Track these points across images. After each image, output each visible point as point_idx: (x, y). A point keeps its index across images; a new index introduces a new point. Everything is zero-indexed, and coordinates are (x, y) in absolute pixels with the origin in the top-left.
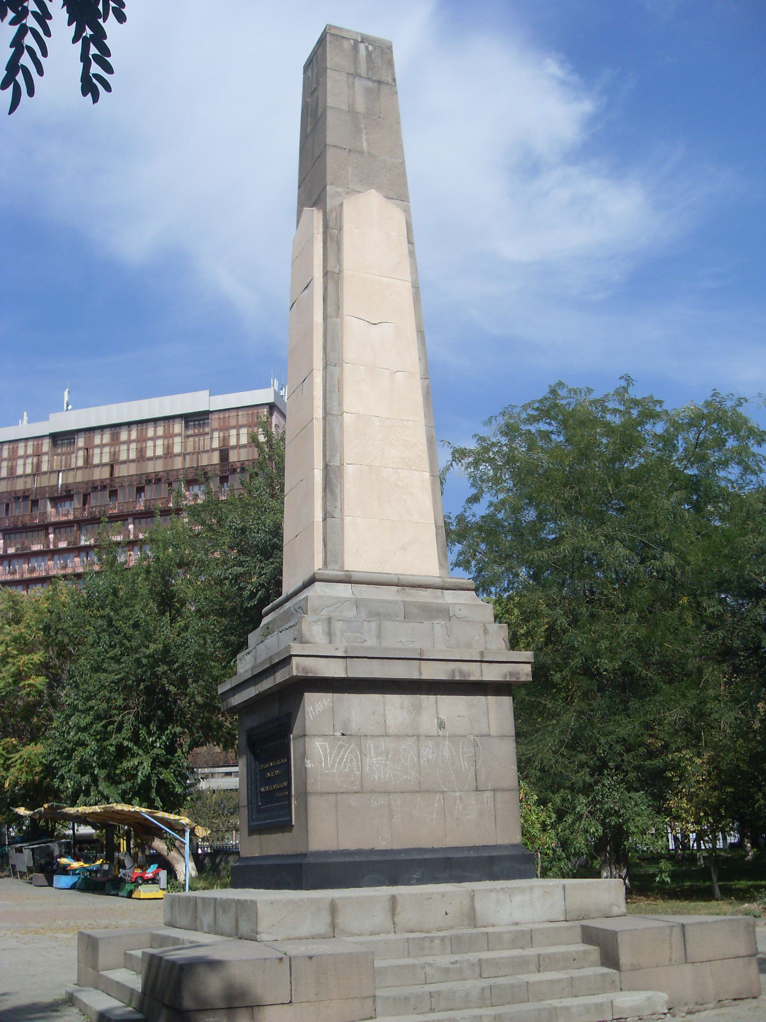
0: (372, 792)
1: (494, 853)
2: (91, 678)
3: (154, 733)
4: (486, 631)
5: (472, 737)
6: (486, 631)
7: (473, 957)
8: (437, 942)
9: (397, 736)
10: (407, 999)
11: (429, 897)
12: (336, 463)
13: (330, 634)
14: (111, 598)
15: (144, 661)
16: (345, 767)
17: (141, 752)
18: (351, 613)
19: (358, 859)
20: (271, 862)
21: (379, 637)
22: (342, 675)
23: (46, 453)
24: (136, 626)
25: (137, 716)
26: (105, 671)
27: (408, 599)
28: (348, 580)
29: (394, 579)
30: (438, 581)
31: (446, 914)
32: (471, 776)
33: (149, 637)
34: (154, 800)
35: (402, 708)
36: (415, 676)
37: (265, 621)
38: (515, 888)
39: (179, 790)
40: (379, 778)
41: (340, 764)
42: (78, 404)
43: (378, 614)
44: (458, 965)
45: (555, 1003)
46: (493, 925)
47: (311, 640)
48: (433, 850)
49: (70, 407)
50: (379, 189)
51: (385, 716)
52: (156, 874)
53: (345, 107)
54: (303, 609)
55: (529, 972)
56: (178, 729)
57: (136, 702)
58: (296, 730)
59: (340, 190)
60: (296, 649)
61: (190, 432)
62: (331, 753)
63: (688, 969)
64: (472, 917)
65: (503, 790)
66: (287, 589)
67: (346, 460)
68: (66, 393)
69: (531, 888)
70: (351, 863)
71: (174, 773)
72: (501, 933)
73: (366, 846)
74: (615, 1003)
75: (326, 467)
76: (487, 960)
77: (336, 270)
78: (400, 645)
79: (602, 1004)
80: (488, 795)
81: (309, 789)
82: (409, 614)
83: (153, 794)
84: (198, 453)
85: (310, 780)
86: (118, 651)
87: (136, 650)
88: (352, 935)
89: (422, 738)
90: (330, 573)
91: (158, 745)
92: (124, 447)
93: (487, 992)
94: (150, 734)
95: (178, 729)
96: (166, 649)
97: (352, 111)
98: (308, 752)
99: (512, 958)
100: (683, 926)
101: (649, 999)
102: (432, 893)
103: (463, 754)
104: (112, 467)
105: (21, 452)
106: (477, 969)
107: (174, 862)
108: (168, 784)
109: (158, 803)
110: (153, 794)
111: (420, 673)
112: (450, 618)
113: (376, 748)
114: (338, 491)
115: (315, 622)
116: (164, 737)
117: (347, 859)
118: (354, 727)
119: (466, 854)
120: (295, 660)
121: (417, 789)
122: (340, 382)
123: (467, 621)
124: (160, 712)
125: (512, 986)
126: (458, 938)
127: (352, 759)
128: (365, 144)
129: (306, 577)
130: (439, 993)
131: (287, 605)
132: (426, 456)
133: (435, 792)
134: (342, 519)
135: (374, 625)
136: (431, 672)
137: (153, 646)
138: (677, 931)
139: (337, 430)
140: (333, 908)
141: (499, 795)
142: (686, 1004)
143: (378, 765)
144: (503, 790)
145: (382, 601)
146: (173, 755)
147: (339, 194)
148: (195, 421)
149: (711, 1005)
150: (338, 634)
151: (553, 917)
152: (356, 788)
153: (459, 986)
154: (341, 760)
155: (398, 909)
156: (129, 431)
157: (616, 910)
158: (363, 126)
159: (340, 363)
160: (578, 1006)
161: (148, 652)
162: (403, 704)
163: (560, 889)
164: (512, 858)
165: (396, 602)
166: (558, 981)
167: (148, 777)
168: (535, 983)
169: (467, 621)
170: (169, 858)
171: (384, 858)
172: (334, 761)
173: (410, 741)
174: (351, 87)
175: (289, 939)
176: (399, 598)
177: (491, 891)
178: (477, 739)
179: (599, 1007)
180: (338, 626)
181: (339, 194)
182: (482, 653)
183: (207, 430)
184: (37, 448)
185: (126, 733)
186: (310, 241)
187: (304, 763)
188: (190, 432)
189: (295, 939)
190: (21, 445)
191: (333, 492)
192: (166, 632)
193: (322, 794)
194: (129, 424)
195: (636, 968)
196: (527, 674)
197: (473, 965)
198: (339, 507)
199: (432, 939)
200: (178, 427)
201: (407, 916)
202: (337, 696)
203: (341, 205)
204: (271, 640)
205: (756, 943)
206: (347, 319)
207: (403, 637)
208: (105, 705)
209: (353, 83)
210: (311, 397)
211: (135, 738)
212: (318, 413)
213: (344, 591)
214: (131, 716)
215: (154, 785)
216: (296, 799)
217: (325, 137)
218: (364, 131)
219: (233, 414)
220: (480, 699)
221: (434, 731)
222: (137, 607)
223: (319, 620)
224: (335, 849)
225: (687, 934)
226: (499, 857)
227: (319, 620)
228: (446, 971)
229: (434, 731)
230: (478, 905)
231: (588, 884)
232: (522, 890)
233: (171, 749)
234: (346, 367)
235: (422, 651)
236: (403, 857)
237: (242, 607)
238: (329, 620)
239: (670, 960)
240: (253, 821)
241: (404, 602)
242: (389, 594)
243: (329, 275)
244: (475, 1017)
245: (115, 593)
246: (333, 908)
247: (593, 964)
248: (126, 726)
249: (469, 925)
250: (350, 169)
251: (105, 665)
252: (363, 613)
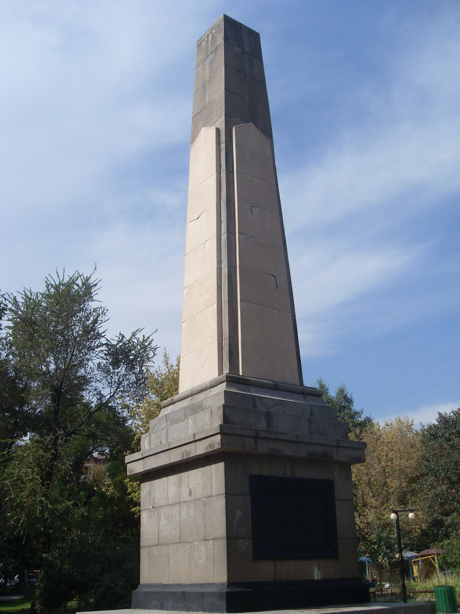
65: (218, 539)
80: (211, 542)
89: (182, 504)
113: (164, 514)
136: (175, 457)
141: (216, 542)
144: (218, 539)
152: (156, 542)
162: (174, 481)
226: (207, 593)
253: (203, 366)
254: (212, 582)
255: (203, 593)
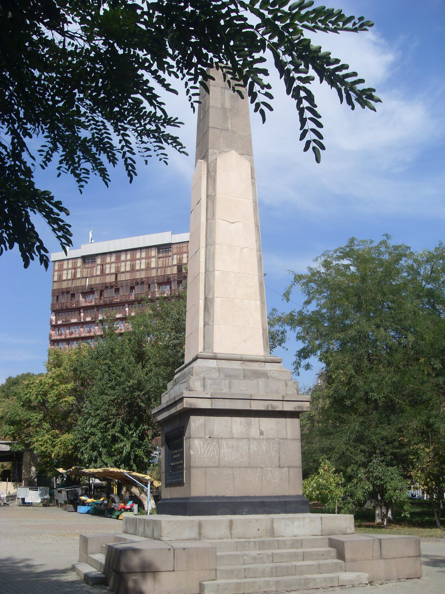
0: (224, 467)
1: (288, 500)
2: (98, 398)
3: (133, 429)
4: (286, 385)
5: (277, 440)
6: (286, 385)
7: (270, 552)
8: (252, 544)
9: (238, 439)
10: (232, 571)
11: (250, 521)
12: (210, 297)
13: (204, 386)
14: (110, 353)
15: (127, 389)
16: (211, 454)
17: (125, 439)
18: (216, 375)
19: (216, 501)
20: (174, 501)
21: (230, 387)
22: (210, 407)
23: (79, 267)
24: (123, 370)
25: (123, 419)
26: (106, 394)
27: (246, 368)
28: (215, 358)
29: (239, 357)
30: (263, 358)
31: (258, 530)
32: (277, 459)
33: (130, 376)
34: (132, 466)
35: (241, 424)
36: (248, 408)
37: (176, 377)
38: (295, 518)
39: (146, 460)
40: (228, 460)
41: (208, 452)
42: (98, 238)
43: (230, 376)
44: (261, 556)
45: (309, 576)
46: (283, 537)
47: (195, 389)
48: (255, 497)
49: (93, 241)
50: (236, 149)
51: (232, 428)
52: (132, 506)
53: (219, 106)
54: (191, 373)
55: (298, 560)
56: (146, 427)
57: (123, 411)
58: (187, 435)
59: (216, 151)
60: (186, 394)
61: (161, 255)
62: (203, 447)
63: (382, 562)
64: (272, 532)
65: (294, 467)
66: (187, 360)
67: (216, 296)
68: (91, 233)
69: (304, 518)
70: (212, 503)
71: (143, 451)
72: (285, 540)
73: (221, 494)
74: (340, 578)
75: (206, 298)
76: (276, 554)
77: (213, 195)
78: (241, 392)
79: (333, 578)
81: (192, 465)
82: (246, 376)
83: (132, 463)
84: (165, 267)
85: (192, 461)
86: (113, 383)
87: (123, 383)
88: (209, 539)
89: (251, 440)
90: (206, 354)
91: (135, 435)
92: (123, 264)
93: (274, 570)
94: (130, 429)
95: (146, 427)
96: (140, 383)
97: (223, 108)
98: (192, 446)
99: (289, 553)
100: (380, 540)
101: (358, 576)
102: (251, 519)
103: (273, 448)
104: (116, 275)
105: (65, 267)
106: (271, 558)
107: (143, 500)
108: (140, 457)
109: (135, 467)
110: (132, 463)
111: (250, 406)
112: (268, 378)
113: (227, 444)
114: (211, 311)
115: (197, 380)
116: (138, 431)
117: (210, 501)
118: (215, 434)
119: (273, 500)
120: (185, 399)
121: (248, 466)
122: (214, 254)
123: (277, 380)
124: (136, 417)
125: (287, 567)
126: (263, 542)
127: (214, 451)
128: (230, 126)
129: (194, 356)
130: (249, 569)
131: (186, 370)
132: (258, 292)
133: (257, 467)
134: (213, 326)
135: (227, 382)
137: (132, 381)
138: (377, 543)
139: (211, 279)
140: (200, 525)
141: (291, 469)
142: (380, 580)
143: (228, 453)
144: (294, 467)
145: (232, 369)
146: (143, 441)
147: (215, 153)
148: (163, 249)
149: (393, 581)
150: (208, 386)
151: (315, 533)
153: (260, 566)
154: (208, 451)
155: (234, 527)
156: (126, 255)
157: (349, 531)
158: (229, 116)
159: (213, 244)
160: (320, 578)
161: (129, 384)
162: (241, 422)
163: (319, 519)
164: (296, 502)
165: (240, 369)
166: (312, 565)
167: (129, 453)
168: (300, 566)
169: (277, 380)
170: (141, 498)
171: (229, 501)
172: (205, 451)
173: (245, 441)
174: (223, 94)
175: (177, 540)
176: (241, 367)
177: (282, 519)
178: (280, 441)
179: (331, 579)
180: (208, 382)
181: (215, 153)
182: (283, 396)
183: (170, 254)
184: (75, 264)
185: (117, 429)
186: (200, 178)
187: (189, 452)
188: (161, 255)
189: (180, 540)
190: (66, 262)
191: (208, 312)
192: (139, 373)
193: (198, 467)
194: (126, 251)
195: (353, 560)
196: (307, 407)
197: (269, 556)
198: (211, 320)
199: (249, 542)
200: (154, 253)
201: (238, 530)
202: (207, 418)
203: (216, 159)
204: (176, 388)
205: (420, 550)
206: (218, 220)
207: (242, 388)
208: (106, 413)
209: (224, 92)
210: (199, 262)
211: (122, 432)
212: (202, 270)
213: (213, 363)
214: (120, 419)
215: (132, 457)
216: (186, 470)
217: (208, 122)
218: (230, 119)
219: (185, 245)
220: (283, 420)
221: (257, 436)
222: (124, 360)
223: (198, 379)
224: (204, 495)
225: (382, 544)
227: (198, 379)
228: (255, 558)
229: (257, 436)
230: (275, 526)
231: (334, 516)
232: (299, 519)
233: (142, 437)
234: (217, 246)
235: (251, 395)
236: (239, 500)
237: (178, 362)
238: (204, 379)
239: (373, 557)
240: (167, 480)
241: (244, 369)
242: (236, 365)
243: (209, 197)
244: (266, 581)
245: (112, 350)
246: (200, 525)
247: (333, 558)
248: (118, 425)
249: (270, 536)
250: (221, 139)
251: (106, 391)
252: (222, 375)
253: (245, 341)
254: (287, 494)
255: (286, 502)
